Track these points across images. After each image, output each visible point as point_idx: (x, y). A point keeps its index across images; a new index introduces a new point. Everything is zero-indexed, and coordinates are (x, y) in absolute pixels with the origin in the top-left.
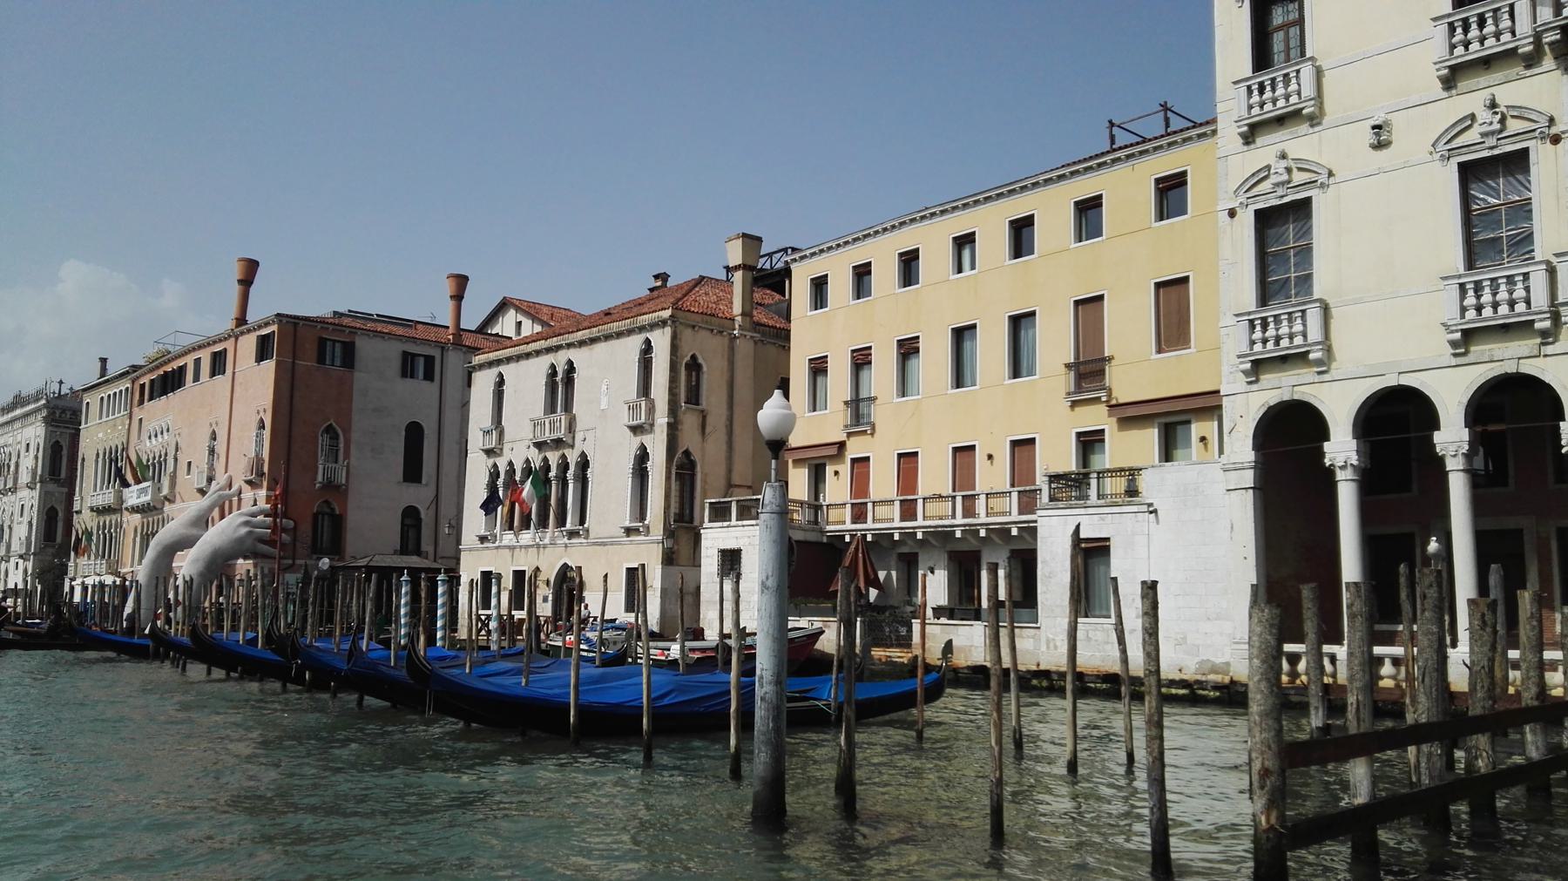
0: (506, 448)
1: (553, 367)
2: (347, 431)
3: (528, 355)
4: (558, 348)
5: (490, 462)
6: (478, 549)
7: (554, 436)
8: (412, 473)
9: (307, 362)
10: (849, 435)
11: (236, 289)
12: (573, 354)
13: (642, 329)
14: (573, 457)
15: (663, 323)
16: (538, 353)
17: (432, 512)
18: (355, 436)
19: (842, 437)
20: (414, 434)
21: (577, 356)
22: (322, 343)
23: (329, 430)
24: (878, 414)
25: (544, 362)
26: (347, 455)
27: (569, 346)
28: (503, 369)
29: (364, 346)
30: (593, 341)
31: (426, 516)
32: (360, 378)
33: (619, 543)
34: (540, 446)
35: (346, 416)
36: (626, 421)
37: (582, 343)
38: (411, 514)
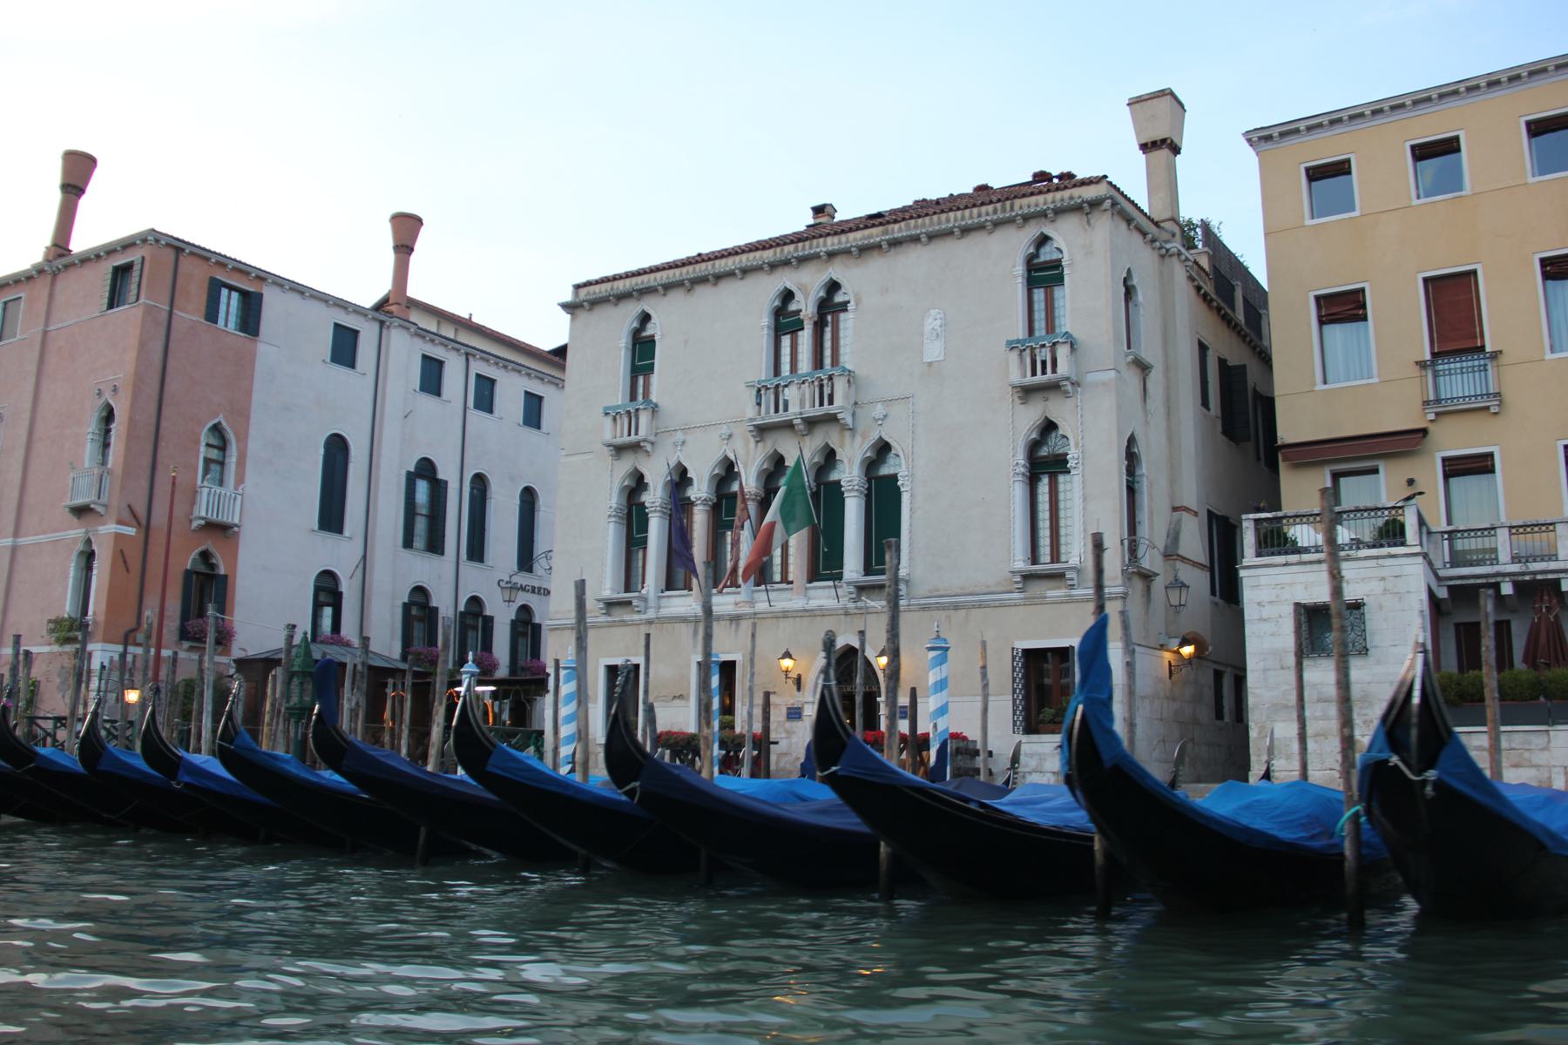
1: (788, 296)
2: (243, 438)
4: (803, 260)
5: (625, 465)
7: (817, 411)
8: (331, 517)
9: (190, 314)
11: (56, 197)
12: (836, 271)
18: (253, 446)
20: (337, 448)
22: (215, 287)
23: (217, 429)
26: (240, 480)
28: (648, 305)
29: (273, 305)
31: (348, 588)
32: (268, 350)
33: (1003, 605)
35: (242, 413)
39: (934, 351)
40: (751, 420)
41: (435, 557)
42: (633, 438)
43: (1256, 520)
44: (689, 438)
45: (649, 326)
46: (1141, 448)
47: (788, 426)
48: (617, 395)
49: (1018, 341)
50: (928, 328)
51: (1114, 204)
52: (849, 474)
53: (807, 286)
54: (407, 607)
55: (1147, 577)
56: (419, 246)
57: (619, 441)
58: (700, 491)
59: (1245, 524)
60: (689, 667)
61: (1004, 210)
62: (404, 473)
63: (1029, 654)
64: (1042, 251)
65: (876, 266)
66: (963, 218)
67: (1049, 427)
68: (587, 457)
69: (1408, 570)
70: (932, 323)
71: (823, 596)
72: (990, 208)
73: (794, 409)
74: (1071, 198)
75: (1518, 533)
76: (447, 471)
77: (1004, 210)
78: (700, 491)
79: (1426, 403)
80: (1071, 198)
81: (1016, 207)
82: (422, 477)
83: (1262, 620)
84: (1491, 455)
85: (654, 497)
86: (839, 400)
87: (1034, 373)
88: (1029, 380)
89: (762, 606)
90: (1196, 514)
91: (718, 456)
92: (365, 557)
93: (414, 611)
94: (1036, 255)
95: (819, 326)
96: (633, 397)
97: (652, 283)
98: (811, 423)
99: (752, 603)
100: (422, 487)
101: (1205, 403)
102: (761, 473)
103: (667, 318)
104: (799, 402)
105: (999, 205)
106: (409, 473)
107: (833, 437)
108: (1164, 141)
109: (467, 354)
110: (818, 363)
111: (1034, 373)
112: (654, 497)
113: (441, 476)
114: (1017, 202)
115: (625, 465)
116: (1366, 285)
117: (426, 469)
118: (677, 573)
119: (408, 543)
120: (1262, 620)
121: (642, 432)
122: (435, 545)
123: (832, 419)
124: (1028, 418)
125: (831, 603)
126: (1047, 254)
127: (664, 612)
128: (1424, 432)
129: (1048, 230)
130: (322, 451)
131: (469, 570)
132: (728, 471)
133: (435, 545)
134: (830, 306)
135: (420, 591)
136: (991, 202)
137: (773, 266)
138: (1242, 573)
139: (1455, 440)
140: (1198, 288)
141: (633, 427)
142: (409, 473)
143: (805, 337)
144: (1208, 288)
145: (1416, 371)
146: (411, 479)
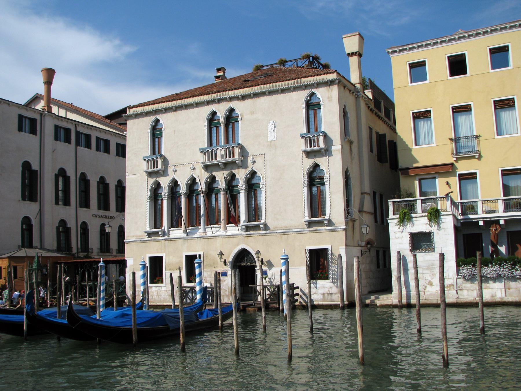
0: (170, 170)
1: (214, 113)
3: (187, 107)
4: (219, 101)
5: (152, 181)
6: (146, 241)
7: (228, 160)
10: (457, 160)
12: (234, 104)
13: (306, 87)
14: (241, 175)
15: (331, 83)
16: (198, 105)
17: (38, 219)
19: (452, 160)
21: (239, 106)
24: (483, 146)
25: (205, 111)
27: (231, 99)
28: (158, 117)
30: (256, 95)
31: (35, 223)
34: (206, 167)
36: (304, 148)
37: (244, 97)
38: (26, 221)
39: (272, 136)
40: (202, 163)
41: (67, 207)
42: (155, 169)
43: (393, 202)
44: (177, 169)
45: (159, 124)
46: (350, 173)
47: (218, 165)
48: (147, 153)
49: (304, 134)
50: (269, 128)
51: (339, 82)
52: (242, 184)
53: (221, 110)
54: (58, 228)
55: (354, 221)
56: (54, 82)
57: (149, 170)
58: (183, 190)
59: (389, 203)
60: (182, 257)
61: (297, 83)
62: (54, 175)
63: (311, 251)
64: (312, 98)
65: (248, 102)
66: (282, 85)
67: (316, 166)
68: (137, 176)
69: (448, 220)
70: (271, 126)
71: (233, 230)
72: (292, 82)
73: (219, 159)
74: (323, 79)
75: (485, 203)
76: (70, 172)
77: (297, 83)
78: (183, 190)
79: (453, 154)
80: (323, 79)
81: (302, 82)
82: (61, 175)
83: (396, 238)
84: (475, 173)
85: (165, 192)
86: (236, 156)
87: (311, 147)
88: (309, 148)
89: (209, 233)
90: (370, 194)
91: (189, 176)
92: (40, 210)
93: (61, 230)
94: (310, 100)
95: (227, 125)
96: (154, 153)
97: (160, 108)
98: (226, 165)
99: (205, 232)
100: (61, 179)
101: (372, 151)
102: (206, 182)
103: (165, 119)
104: (220, 156)
105: (296, 81)
106: (56, 175)
107: (235, 171)
108: (356, 53)
109: (76, 125)
110: (227, 141)
111: (311, 147)
112: (165, 192)
113: (68, 174)
114: (303, 79)
115: (152, 181)
116: (431, 109)
117: (62, 173)
118: (175, 223)
119: (57, 203)
120: (396, 238)
121: (159, 167)
122: (67, 202)
123: (234, 163)
124: (309, 162)
125: (237, 232)
126: (313, 101)
127: (171, 236)
128: (452, 164)
129: (314, 91)
130: (21, 169)
131: (82, 211)
132: (192, 182)
133: (67, 202)
134: (231, 118)
135: (63, 223)
136: (292, 79)
137: (208, 103)
138: (389, 221)
139: (463, 167)
140: (369, 107)
141: (155, 164)
142: (56, 175)
143: (222, 129)
144: (372, 106)
145: (450, 142)
146: (57, 177)
